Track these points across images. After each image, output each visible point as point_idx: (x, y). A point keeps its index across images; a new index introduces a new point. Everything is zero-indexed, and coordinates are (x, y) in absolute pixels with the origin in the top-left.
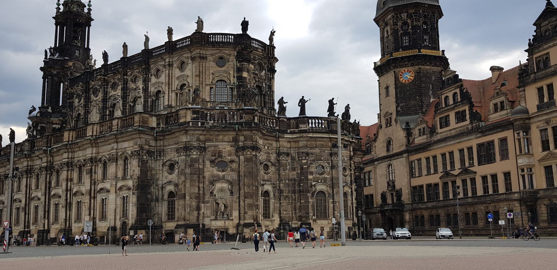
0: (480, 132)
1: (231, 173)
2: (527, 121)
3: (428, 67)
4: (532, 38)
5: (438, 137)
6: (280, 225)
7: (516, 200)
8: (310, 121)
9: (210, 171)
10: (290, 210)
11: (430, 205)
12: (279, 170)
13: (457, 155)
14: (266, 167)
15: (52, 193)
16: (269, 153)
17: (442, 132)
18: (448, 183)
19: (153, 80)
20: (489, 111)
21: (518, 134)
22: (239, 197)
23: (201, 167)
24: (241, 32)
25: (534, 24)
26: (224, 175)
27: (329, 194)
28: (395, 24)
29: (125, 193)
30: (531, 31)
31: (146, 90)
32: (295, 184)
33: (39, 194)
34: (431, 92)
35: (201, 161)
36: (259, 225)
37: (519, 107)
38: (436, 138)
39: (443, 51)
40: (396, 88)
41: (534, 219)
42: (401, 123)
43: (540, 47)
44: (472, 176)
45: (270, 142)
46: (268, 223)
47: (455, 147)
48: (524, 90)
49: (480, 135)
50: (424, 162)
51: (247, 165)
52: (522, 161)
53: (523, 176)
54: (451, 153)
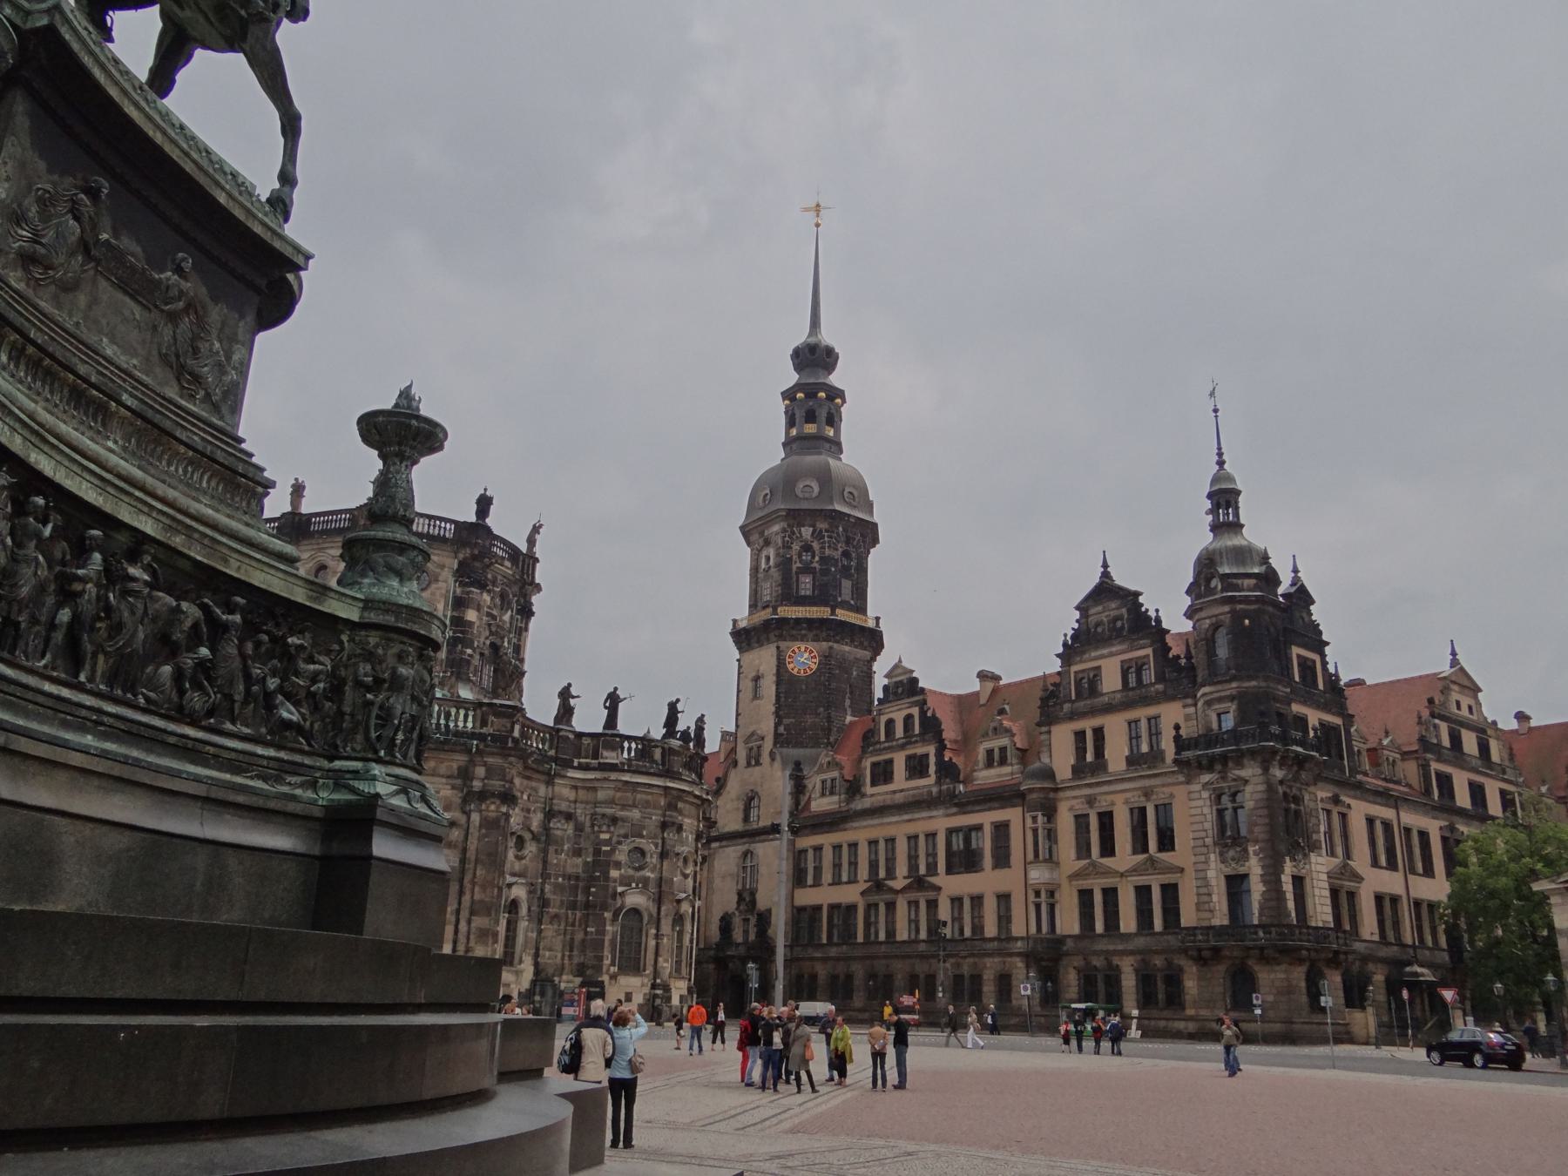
0: (956, 805)
2: (1052, 795)
3: (847, 648)
4: (1071, 632)
5: (866, 803)
6: (534, 983)
7: (1019, 954)
8: (626, 744)
10: (559, 947)
11: (833, 952)
12: (545, 852)
13: (902, 848)
14: (520, 843)
16: (528, 811)
17: (874, 794)
18: (877, 905)
20: (976, 763)
21: (1034, 819)
22: (458, 912)
24: (473, 519)
25: (1077, 608)
28: (787, 546)
30: (1069, 621)
32: (577, 887)
34: (848, 702)
37: (1037, 765)
38: (859, 805)
39: (878, 619)
40: (778, 683)
41: (1051, 997)
42: (784, 763)
43: (1084, 652)
44: (931, 895)
45: (534, 784)
47: (899, 828)
48: (1049, 732)
49: (954, 810)
50: (828, 855)
51: (486, 836)
52: (1038, 875)
53: (1038, 906)
54: (891, 841)
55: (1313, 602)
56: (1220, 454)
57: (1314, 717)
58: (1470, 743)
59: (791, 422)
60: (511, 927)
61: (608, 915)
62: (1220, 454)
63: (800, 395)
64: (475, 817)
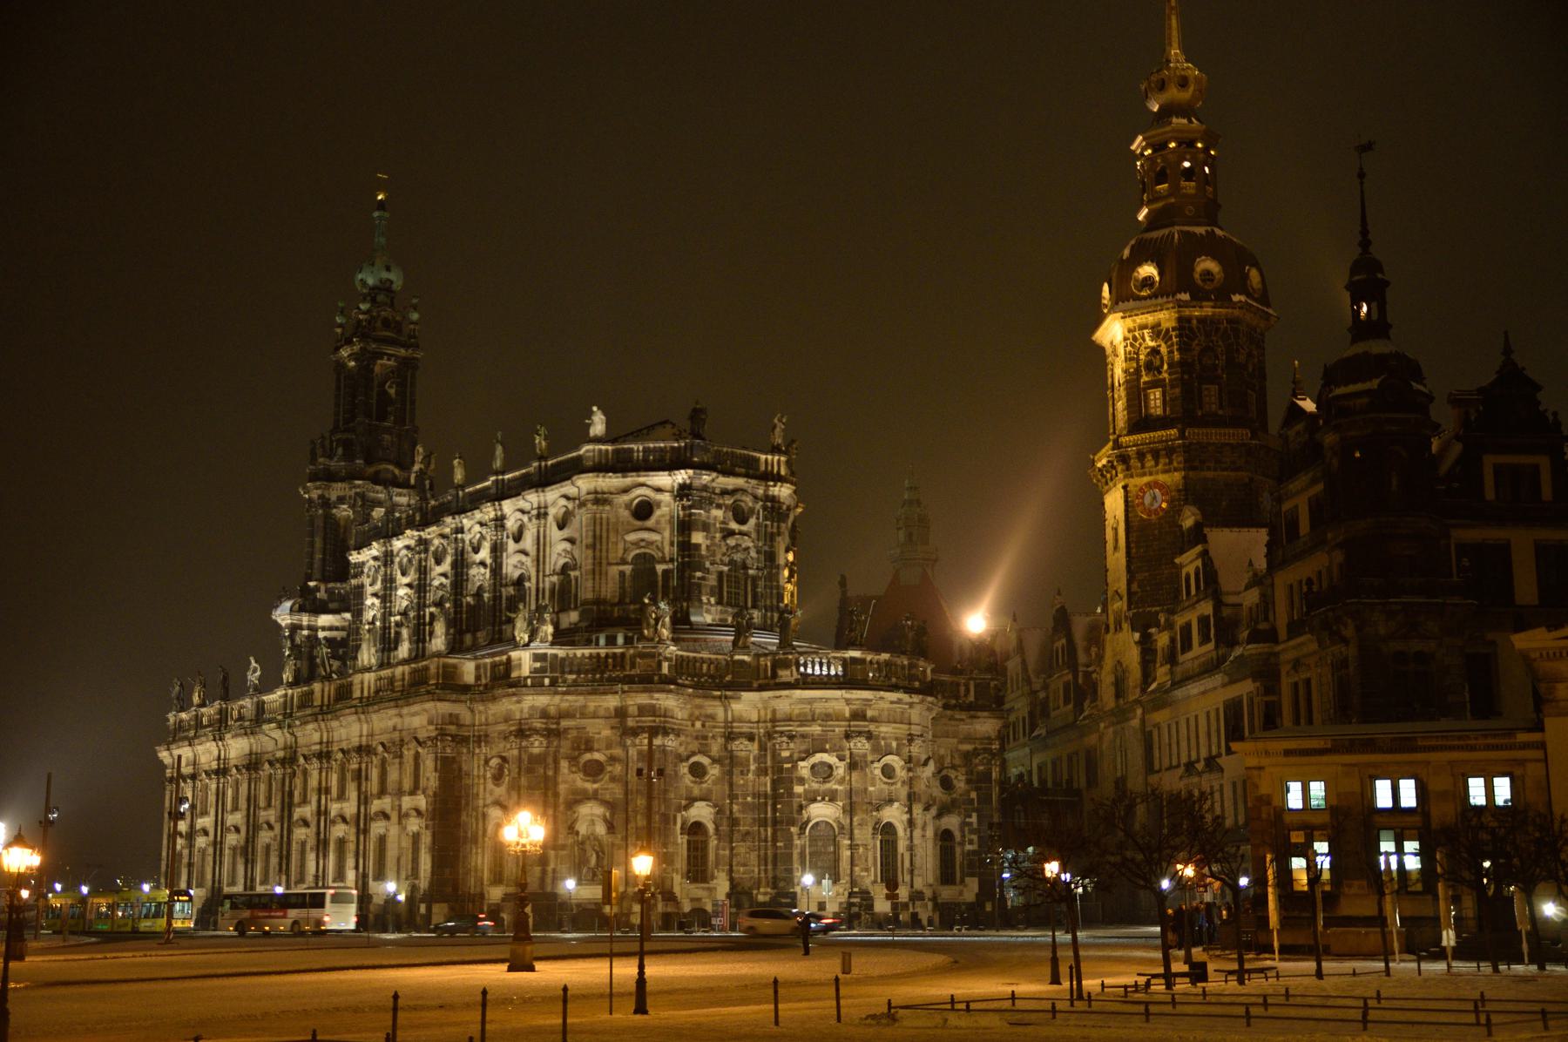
1: (611, 785)
3: (1210, 474)
12: (730, 773)
15: (296, 817)
16: (705, 738)
19: (511, 546)
23: (550, 773)
26: (596, 791)
27: (842, 827)
29: (414, 825)
31: (496, 570)
35: (550, 760)
46: (697, 890)
55: (1538, 388)
56: (1364, 232)
57: (1522, 542)
61: (794, 830)
64: (633, 752)
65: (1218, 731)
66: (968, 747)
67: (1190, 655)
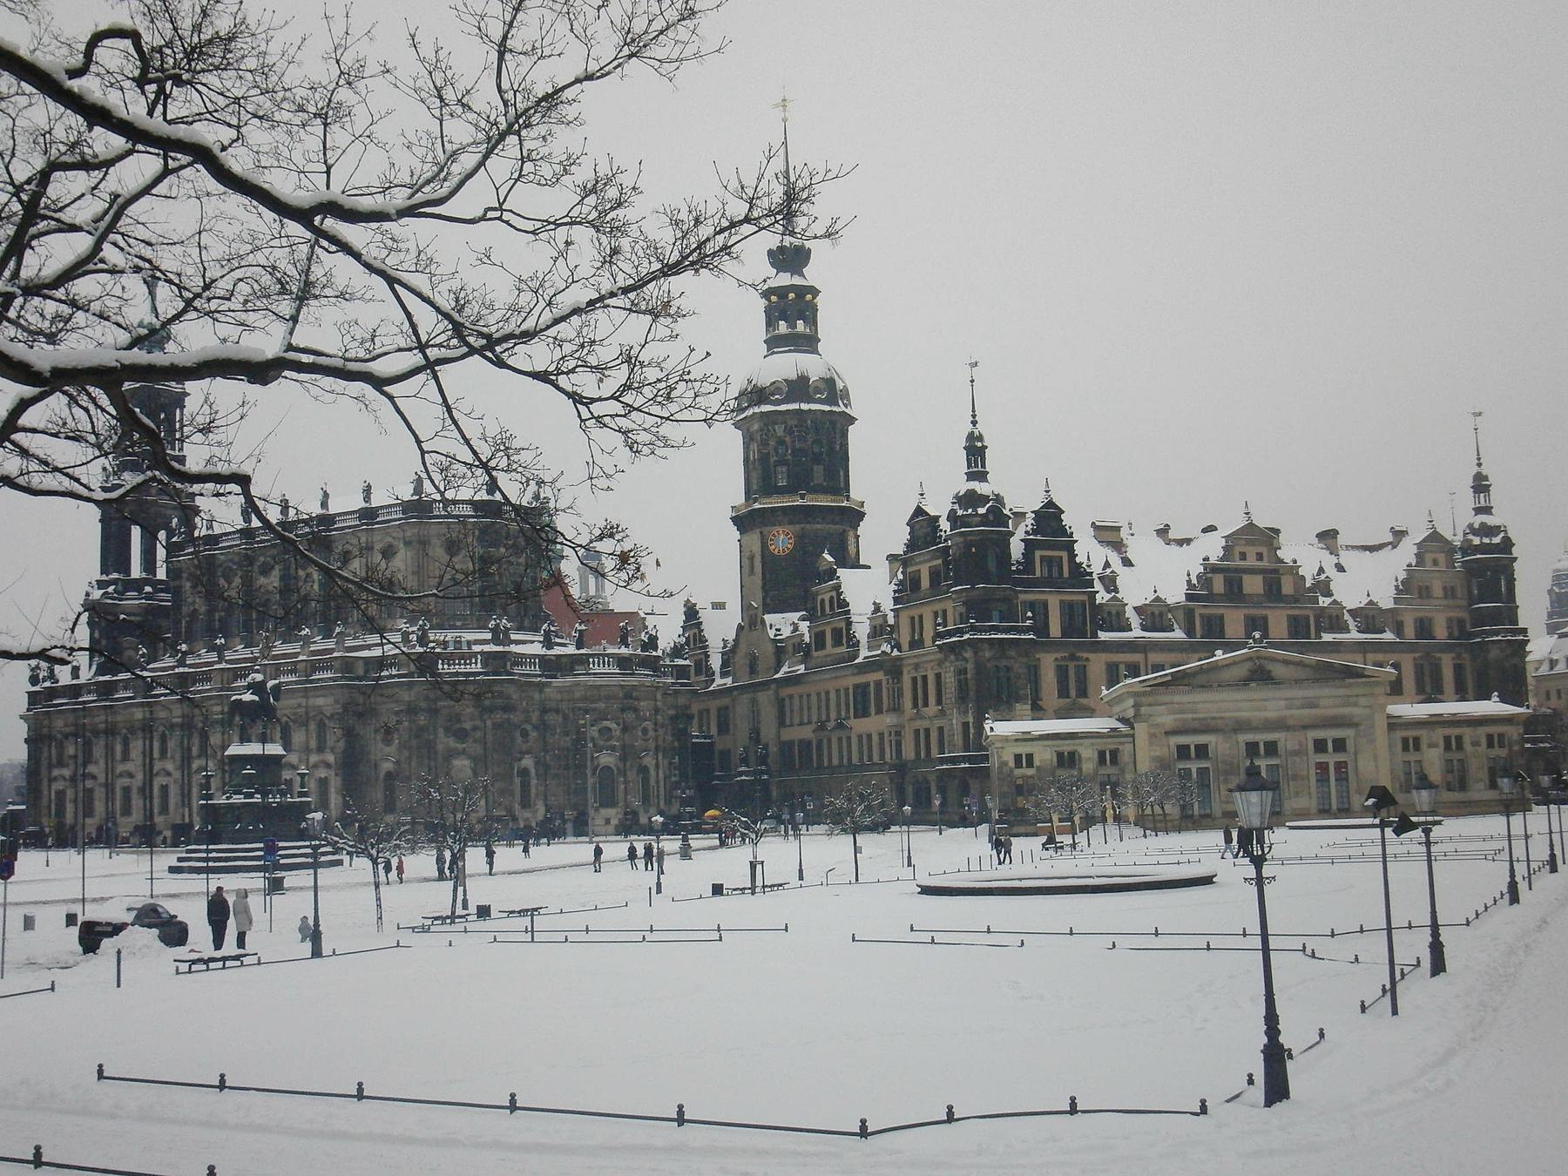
9: (444, 741)
13: (833, 696)
15: (195, 766)
28: (764, 443)
30: (904, 534)
33: (170, 766)
36: (515, 819)
46: (527, 814)
54: (827, 693)
56: (974, 416)
58: (1253, 585)
59: (770, 323)
60: (525, 786)
62: (974, 416)
63: (774, 298)
64: (489, 723)
65: (847, 705)
66: (672, 712)
67: (820, 653)
